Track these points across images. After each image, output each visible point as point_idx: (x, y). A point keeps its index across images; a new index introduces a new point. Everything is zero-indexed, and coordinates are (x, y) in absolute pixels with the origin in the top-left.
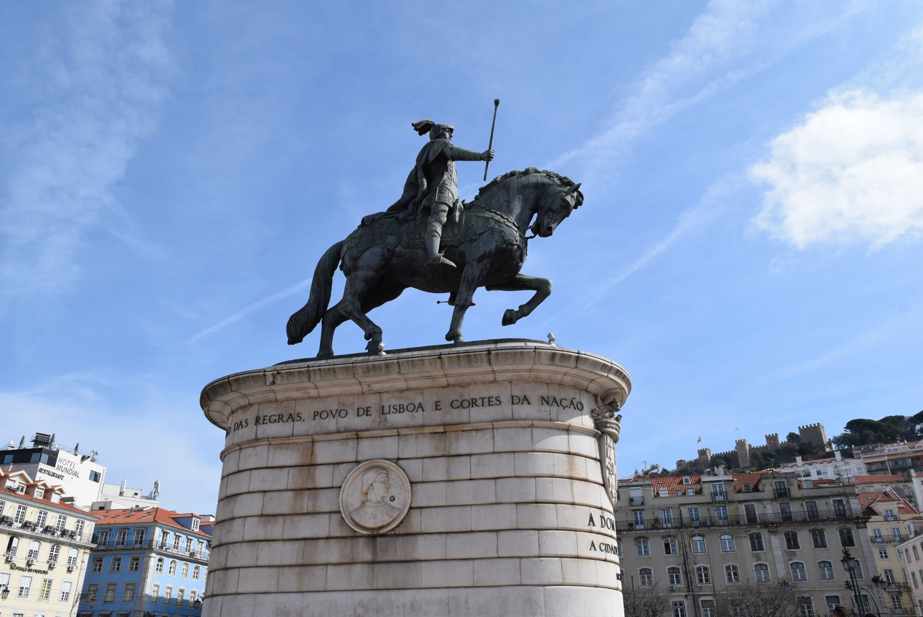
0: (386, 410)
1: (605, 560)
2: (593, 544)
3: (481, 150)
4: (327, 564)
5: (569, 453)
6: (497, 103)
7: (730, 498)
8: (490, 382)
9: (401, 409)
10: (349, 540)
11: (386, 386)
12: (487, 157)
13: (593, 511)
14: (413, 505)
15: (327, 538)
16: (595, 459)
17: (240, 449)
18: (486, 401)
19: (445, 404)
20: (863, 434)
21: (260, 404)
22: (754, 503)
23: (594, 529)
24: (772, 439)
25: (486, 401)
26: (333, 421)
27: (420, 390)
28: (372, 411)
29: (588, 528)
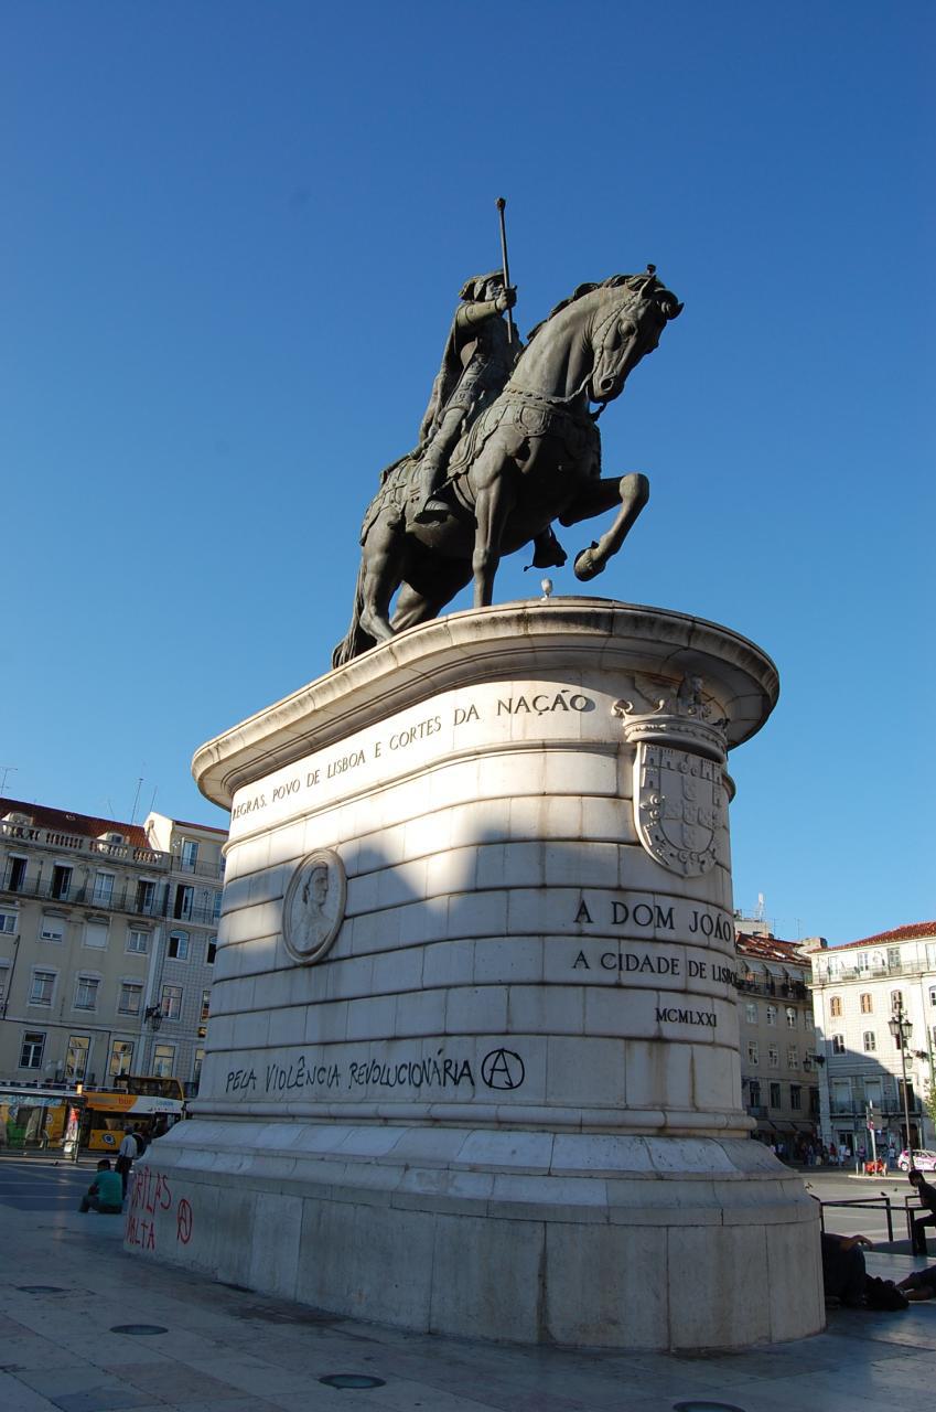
0: (332, 773)
1: (618, 986)
2: (582, 957)
4: (271, 1009)
5: (544, 794)
6: (502, 204)
9: (344, 765)
10: (290, 971)
13: (588, 895)
14: (348, 913)
15: (275, 971)
16: (616, 796)
18: (425, 726)
23: (587, 928)
25: (425, 726)
29: (574, 928)
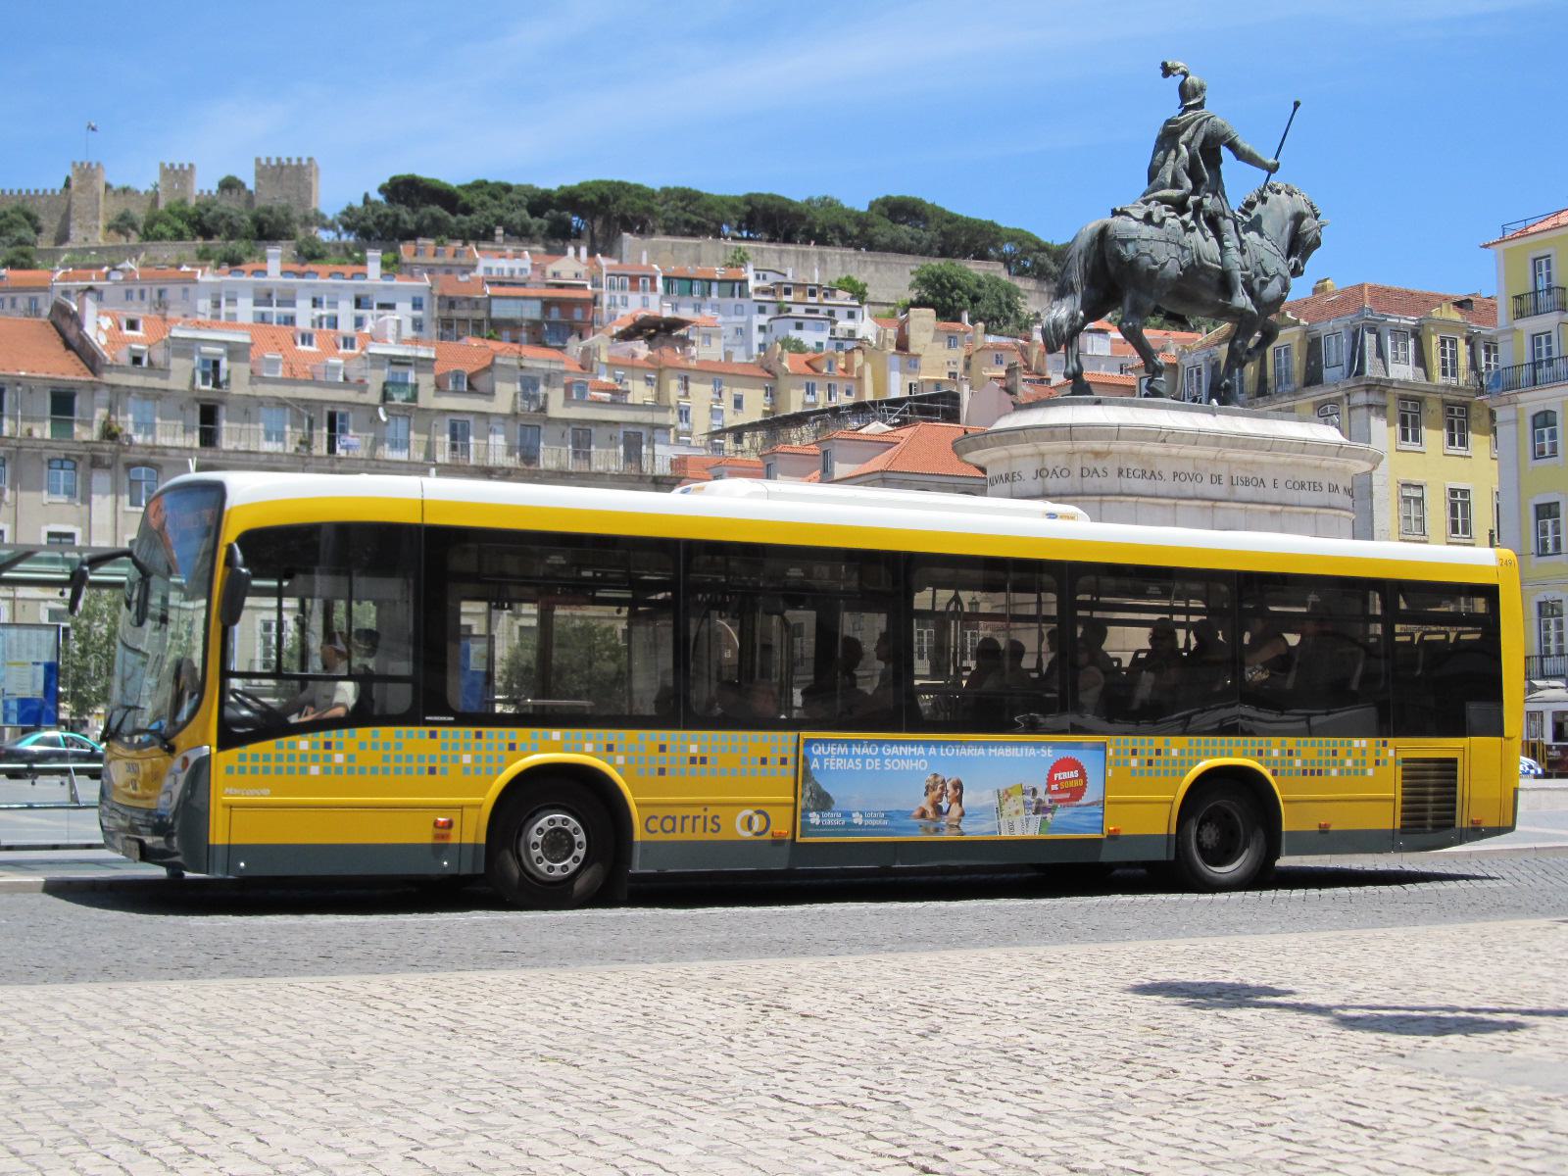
3: (1271, 161)
6: (1297, 104)
7: (422, 403)
8: (1316, 467)
9: (1246, 482)
11: (1237, 455)
12: (1272, 169)
17: (1101, 502)
19: (1281, 483)
20: (417, 213)
21: (1119, 453)
22: (471, 418)
24: (177, 175)
26: (1191, 484)
27: (1261, 465)
28: (1224, 479)
